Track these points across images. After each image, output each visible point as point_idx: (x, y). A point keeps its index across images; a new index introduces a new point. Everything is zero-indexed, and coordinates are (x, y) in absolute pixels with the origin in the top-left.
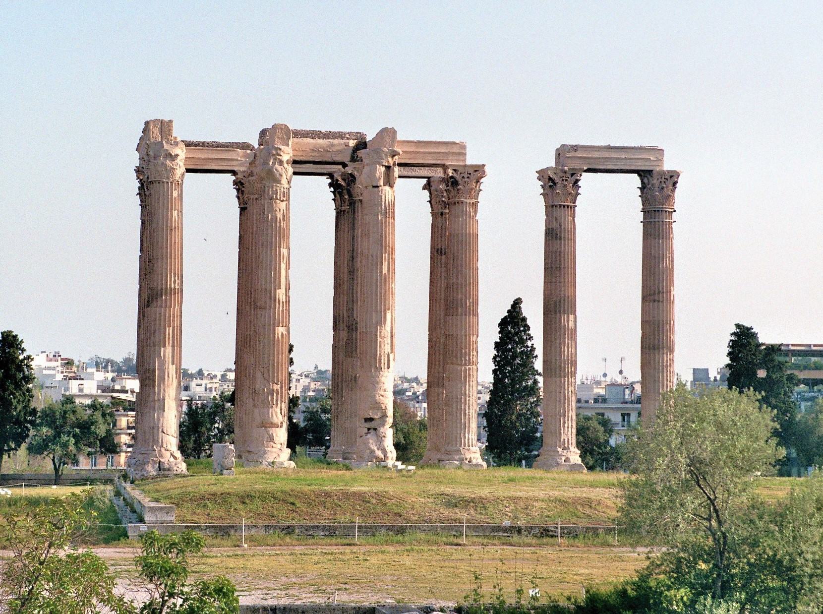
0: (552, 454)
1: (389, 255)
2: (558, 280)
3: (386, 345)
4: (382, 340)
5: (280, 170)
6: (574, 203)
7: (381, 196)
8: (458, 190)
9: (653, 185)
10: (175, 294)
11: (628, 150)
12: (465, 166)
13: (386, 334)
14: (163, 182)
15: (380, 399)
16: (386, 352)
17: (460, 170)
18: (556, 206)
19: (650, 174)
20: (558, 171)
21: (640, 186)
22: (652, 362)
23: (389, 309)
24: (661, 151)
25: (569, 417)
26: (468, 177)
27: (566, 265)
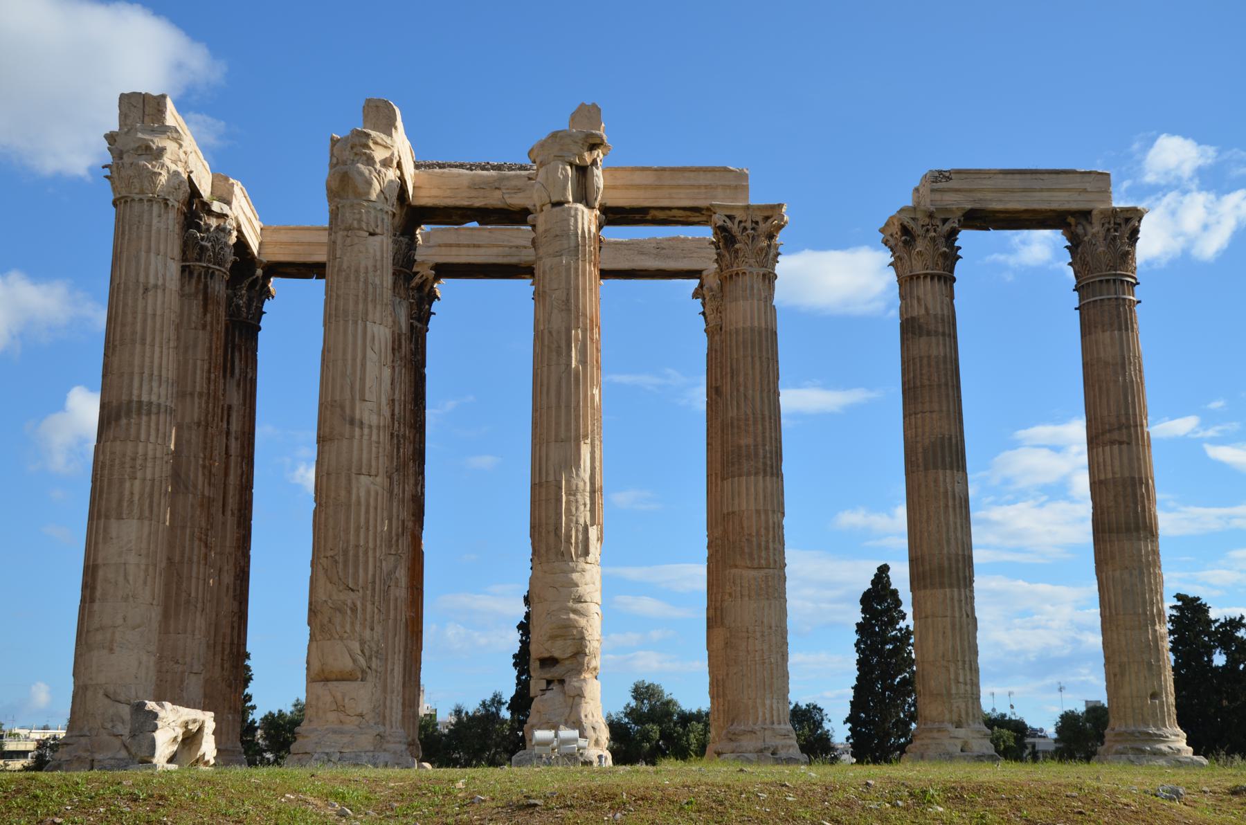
0: (936, 735)
1: (584, 331)
3: (582, 508)
4: (572, 498)
5: (367, 172)
6: (952, 270)
7: (568, 221)
8: (736, 251)
9: (1094, 235)
10: (149, 413)
11: (1046, 176)
12: (748, 207)
13: (581, 484)
14: (133, 200)
15: (569, 619)
16: (582, 521)
17: (739, 215)
18: (918, 277)
19: (1087, 220)
20: (919, 215)
23: (586, 437)
24: (1105, 176)
25: (964, 662)
26: (753, 229)
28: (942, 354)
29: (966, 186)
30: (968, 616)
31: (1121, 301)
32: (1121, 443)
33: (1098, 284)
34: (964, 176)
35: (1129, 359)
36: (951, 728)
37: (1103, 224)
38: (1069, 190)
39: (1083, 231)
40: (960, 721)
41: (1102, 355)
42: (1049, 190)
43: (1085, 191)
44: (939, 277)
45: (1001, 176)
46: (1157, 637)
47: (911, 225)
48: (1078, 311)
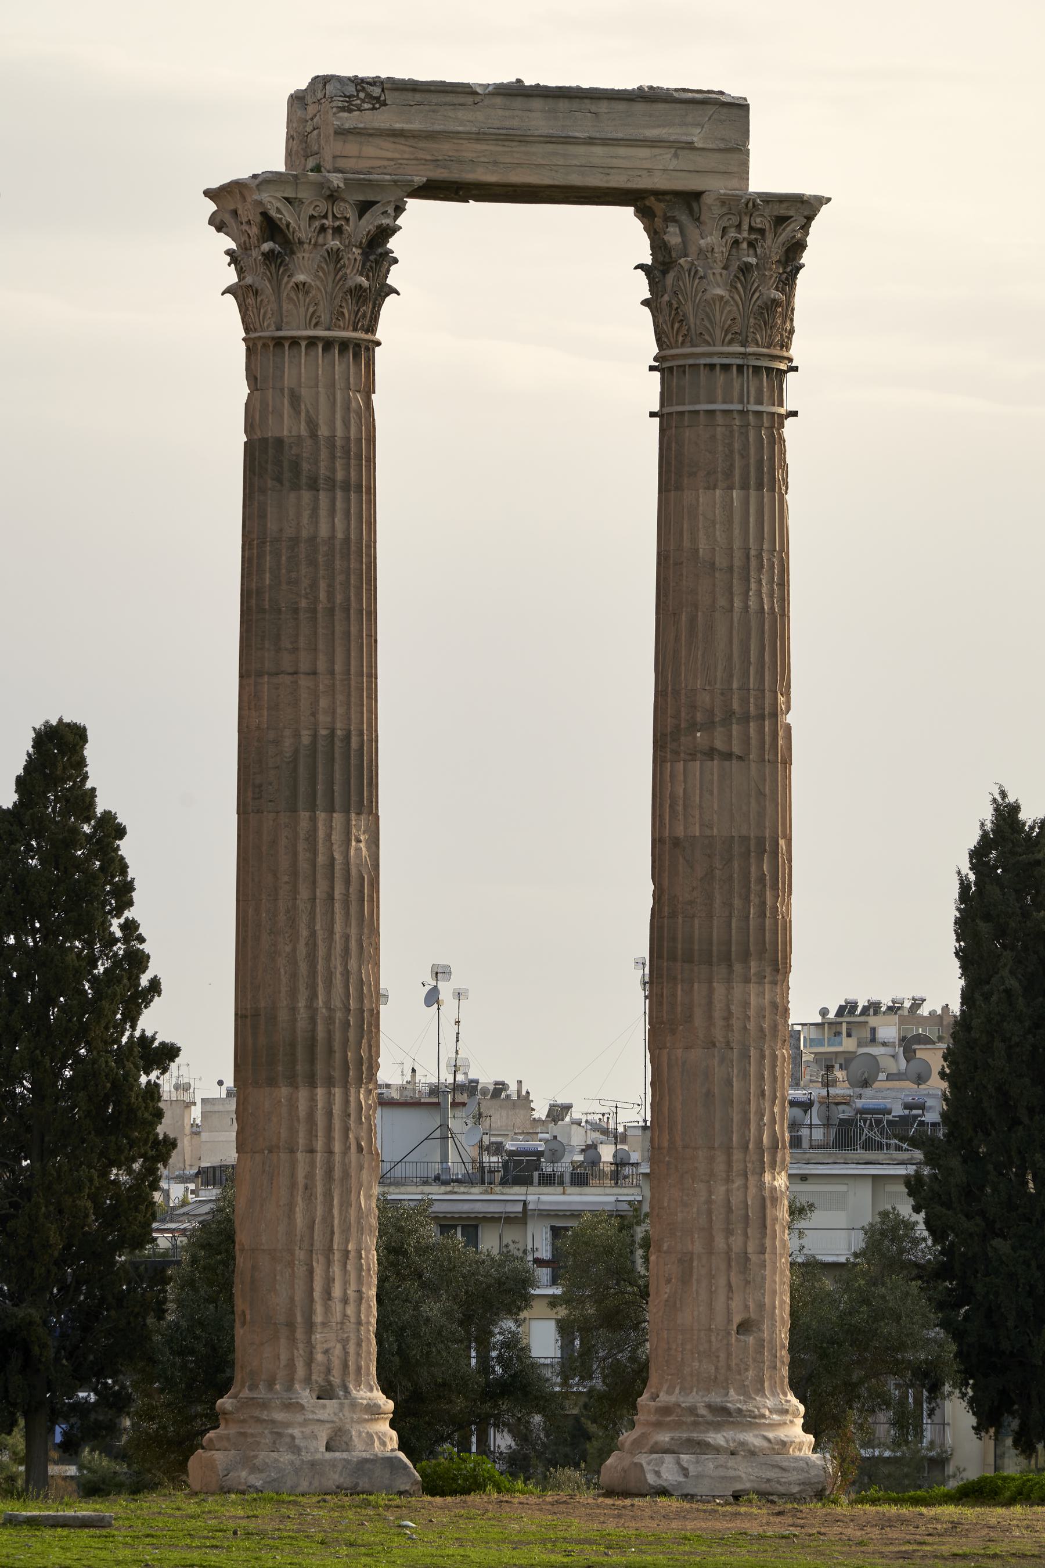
0: (279, 1416)
2: (304, 667)
6: (372, 328)
11: (603, 107)
18: (295, 342)
20: (304, 194)
21: (648, 260)
22: (698, 1013)
27: (339, 598)
28: (340, 535)
29: (416, 126)
30: (360, 1149)
31: (751, 418)
32: (728, 756)
33: (703, 373)
34: (418, 97)
35: (759, 557)
36: (305, 1396)
37: (724, 230)
38: (653, 143)
39: (679, 240)
40: (330, 1383)
41: (703, 546)
42: (606, 142)
43: (690, 146)
44: (344, 345)
45: (498, 100)
46: (764, 1199)
47: (286, 216)
48: (656, 421)
